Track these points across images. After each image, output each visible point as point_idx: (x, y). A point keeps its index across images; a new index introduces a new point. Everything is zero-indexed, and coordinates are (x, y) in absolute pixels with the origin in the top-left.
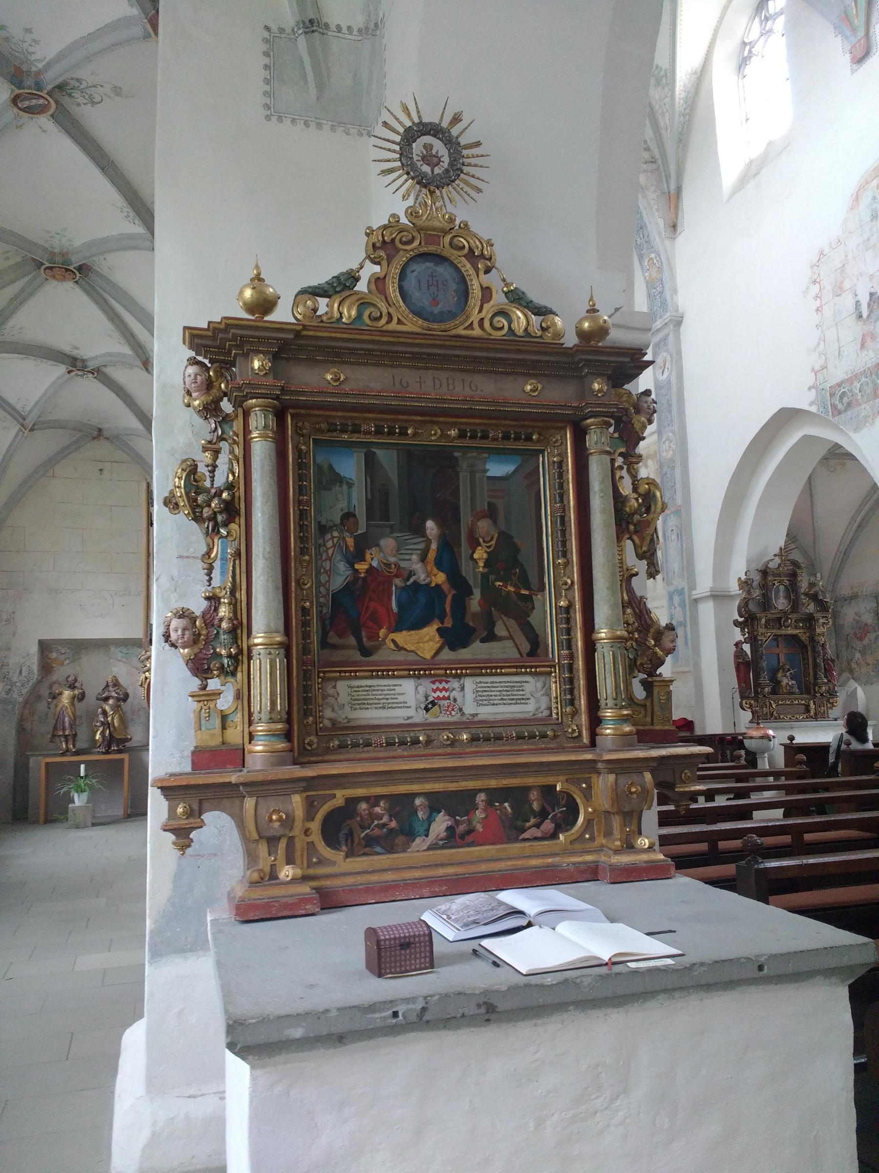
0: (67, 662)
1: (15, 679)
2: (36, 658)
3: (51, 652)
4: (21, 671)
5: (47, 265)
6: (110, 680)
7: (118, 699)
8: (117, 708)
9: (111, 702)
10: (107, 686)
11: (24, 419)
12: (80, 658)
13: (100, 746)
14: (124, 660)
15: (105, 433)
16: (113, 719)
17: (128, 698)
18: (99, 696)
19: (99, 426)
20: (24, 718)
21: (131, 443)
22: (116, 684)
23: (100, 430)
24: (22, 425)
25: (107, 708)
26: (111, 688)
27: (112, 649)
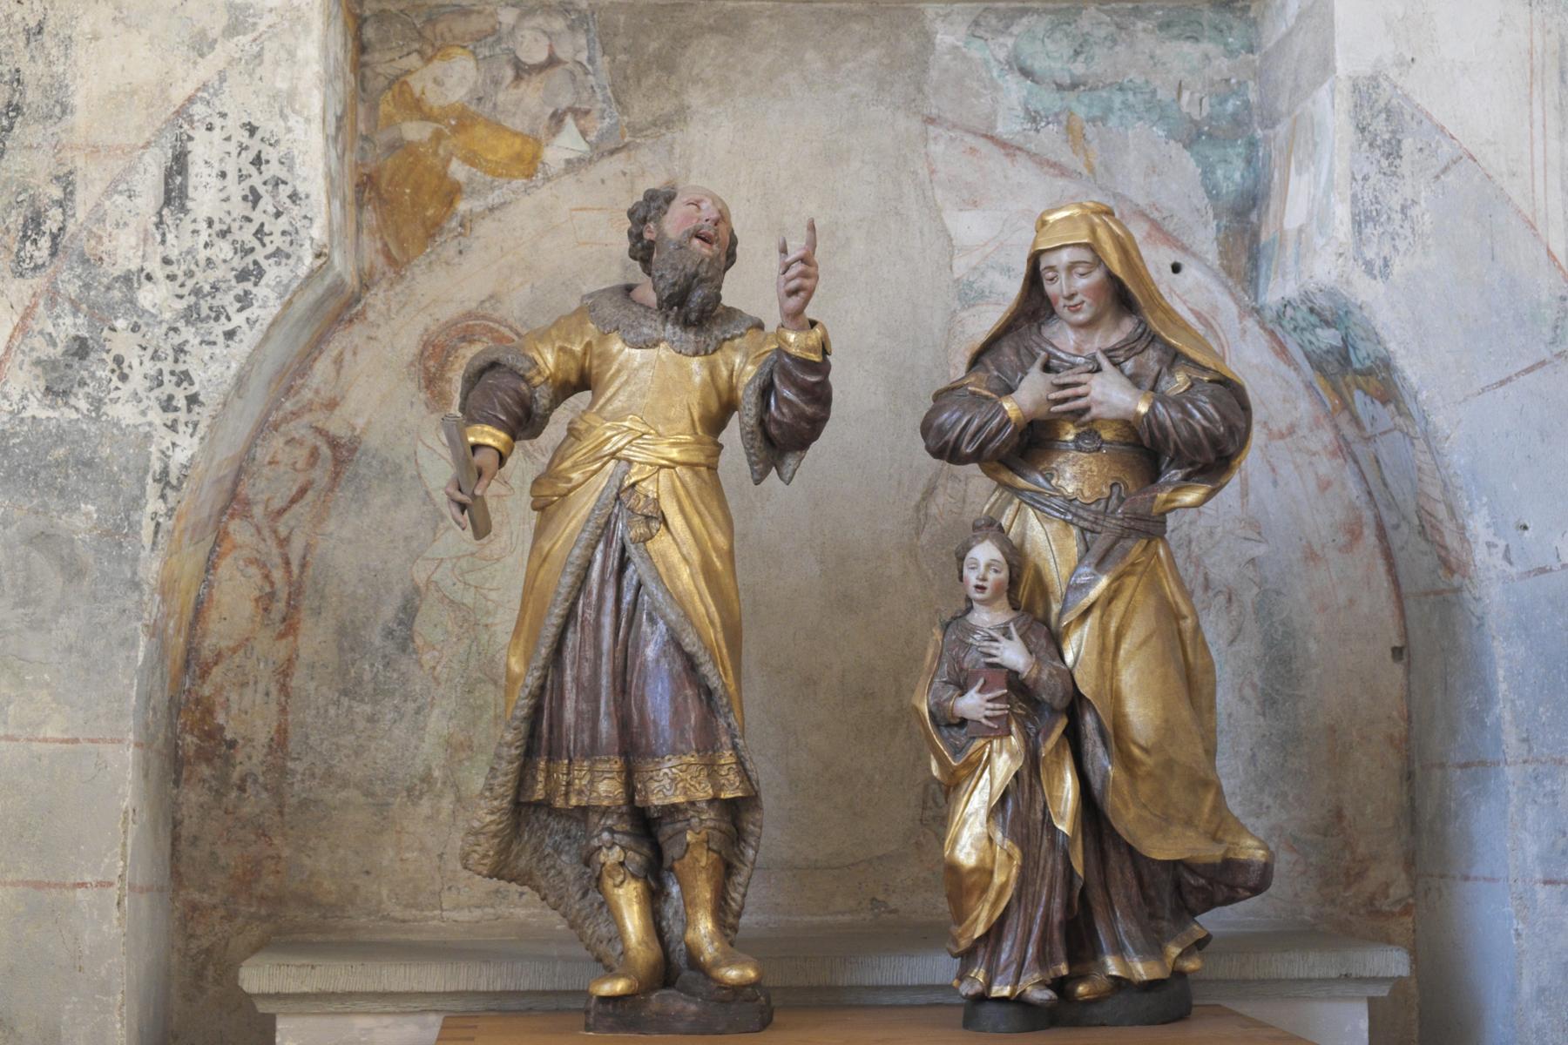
0: (568, 143)
3: (433, 49)
4: (179, 163)
13: (996, 932)
14: (1050, 139)
16: (1108, 650)
20: (206, 653)
27: (948, 36)
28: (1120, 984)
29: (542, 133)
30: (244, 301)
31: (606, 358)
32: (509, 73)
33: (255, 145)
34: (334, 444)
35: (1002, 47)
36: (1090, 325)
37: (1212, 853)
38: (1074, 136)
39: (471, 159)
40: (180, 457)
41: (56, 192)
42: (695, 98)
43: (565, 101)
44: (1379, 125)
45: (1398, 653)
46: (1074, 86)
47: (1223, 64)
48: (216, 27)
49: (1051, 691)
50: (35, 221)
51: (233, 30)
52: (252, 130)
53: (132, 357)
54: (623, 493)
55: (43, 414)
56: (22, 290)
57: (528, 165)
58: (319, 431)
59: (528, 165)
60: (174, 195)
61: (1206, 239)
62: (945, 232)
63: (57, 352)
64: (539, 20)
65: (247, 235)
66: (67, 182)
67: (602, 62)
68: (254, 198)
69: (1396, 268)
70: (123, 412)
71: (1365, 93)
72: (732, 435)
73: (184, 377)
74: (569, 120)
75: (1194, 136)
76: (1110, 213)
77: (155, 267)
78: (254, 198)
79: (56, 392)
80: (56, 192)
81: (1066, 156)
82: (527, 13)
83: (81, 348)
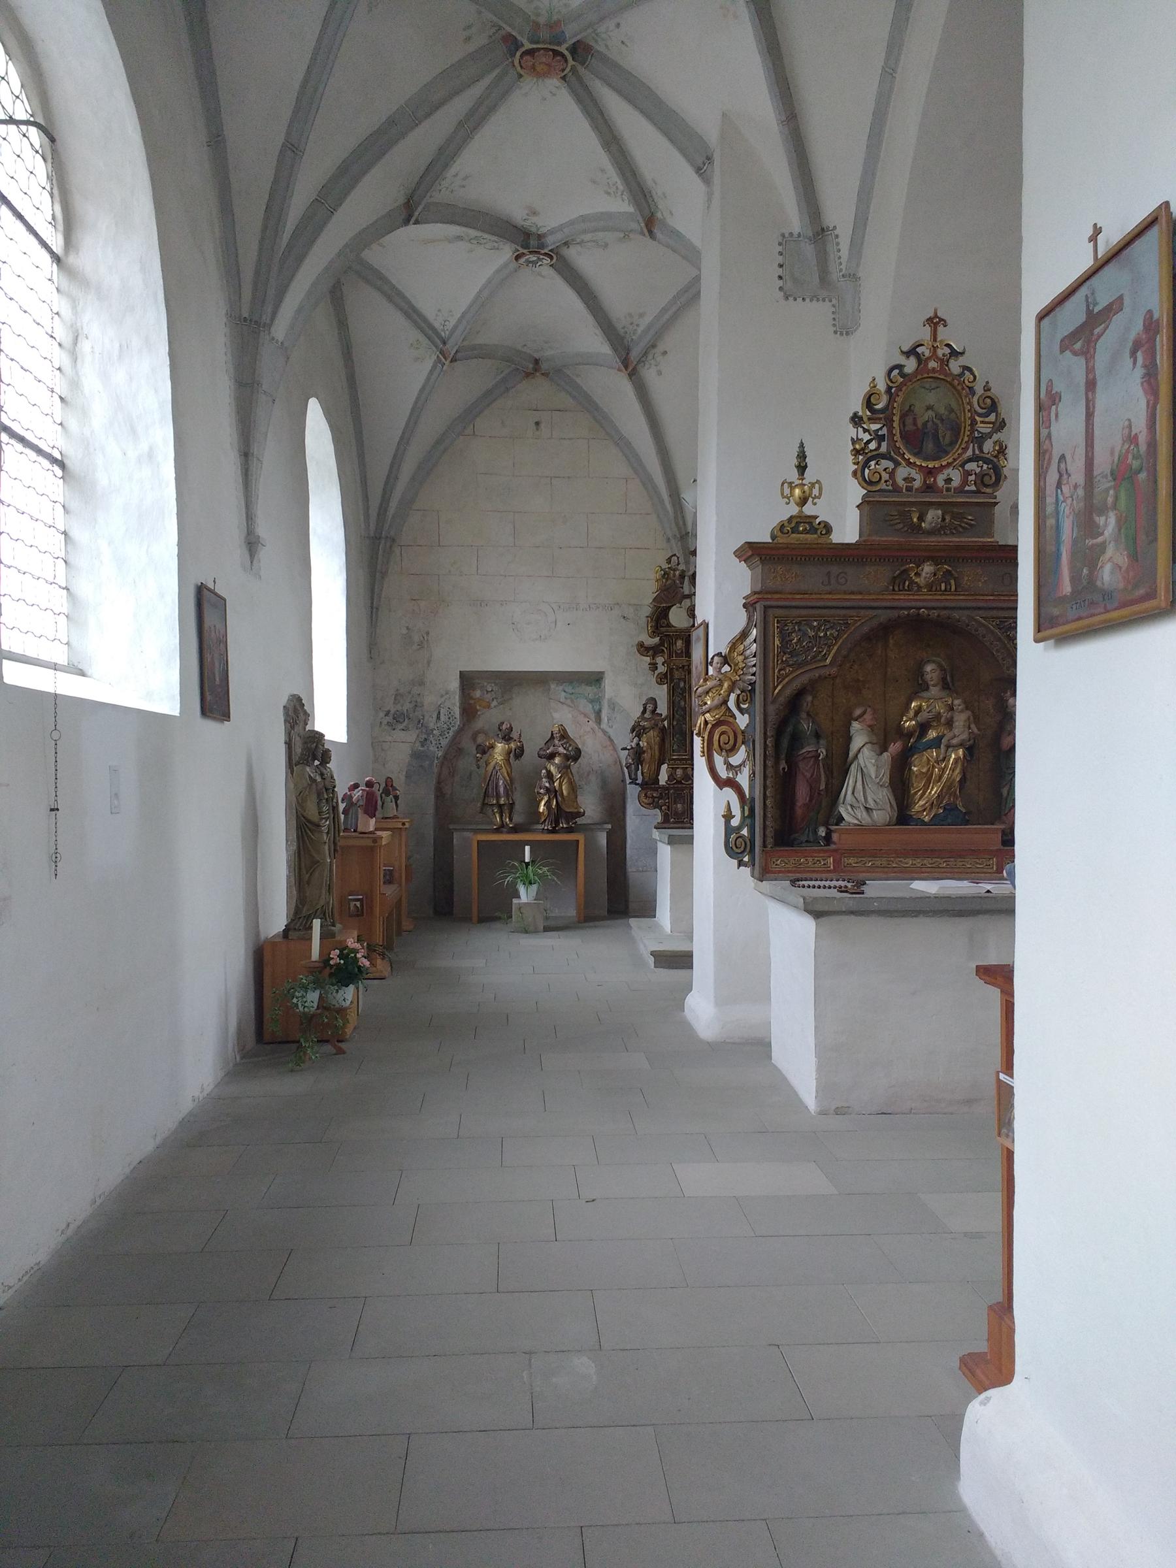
0: (495, 703)
1: (431, 725)
2: (457, 697)
5: (528, 46)
6: (556, 730)
7: (567, 758)
8: (565, 769)
9: (557, 760)
10: (552, 737)
11: (444, 343)
12: (511, 699)
13: (545, 820)
14: (569, 702)
15: (544, 366)
16: (561, 785)
17: (580, 756)
18: (542, 753)
19: (536, 355)
21: (578, 380)
22: (564, 735)
23: (537, 361)
24: (442, 352)
25: (553, 769)
26: (556, 742)
27: (553, 686)
28: (562, 828)
29: (491, 702)
30: (448, 733)
31: (495, 745)
32: (486, 693)
33: (450, 711)
34: (460, 749)
35: (561, 688)
36: (559, 741)
37: (576, 810)
38: (572, 701)
39: (480, 706)
40: (439, 755)
41: (422, 717)
42: (514, 696)
43: (494, 696)
44: (612, 706)
45: (622, 781)
46: (572, 694)
47: (595, 690)
48: (444, 693)
49: (552, 789)
50: (419, 722)
51: (447, 693)
52: (449, 708)
53: (433, 741)
54: (497, 763)
55: (421, 749)
56: (417, 731)
57: (489, 707)
58: (458, 747)
59: (489, 707)
60: (438, 718)
61: (593, 716)
62: (552, 716)
63: (422, 740)
64: (490, 684)
65: (448, 724)
66: (423, 716)
67: (500, 691)
68: (449, 718)
69: (614, 727)
70: (431, 748)
71: (610, 700)
72: (511, 755)
73: (440, 744)
74: (495, 700)
75: (592, 701)
76: (562, 725)
77: (436, 728)
78: (449, 718)
79: (422, 746)
80: (422, 717)
81: (571, 704)
82: (489, 683)
83: (426, 739)
